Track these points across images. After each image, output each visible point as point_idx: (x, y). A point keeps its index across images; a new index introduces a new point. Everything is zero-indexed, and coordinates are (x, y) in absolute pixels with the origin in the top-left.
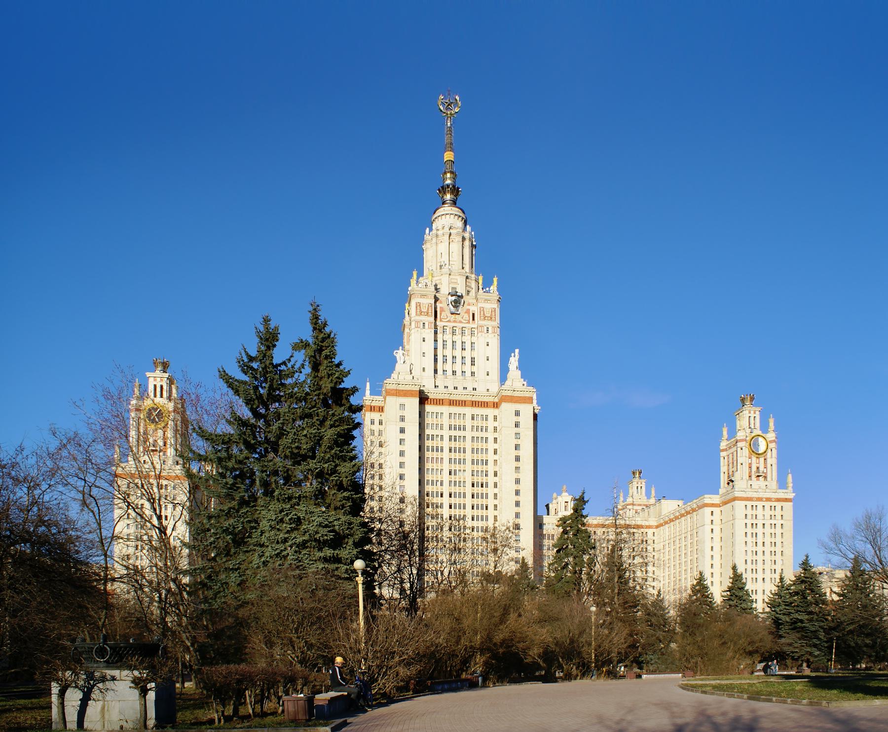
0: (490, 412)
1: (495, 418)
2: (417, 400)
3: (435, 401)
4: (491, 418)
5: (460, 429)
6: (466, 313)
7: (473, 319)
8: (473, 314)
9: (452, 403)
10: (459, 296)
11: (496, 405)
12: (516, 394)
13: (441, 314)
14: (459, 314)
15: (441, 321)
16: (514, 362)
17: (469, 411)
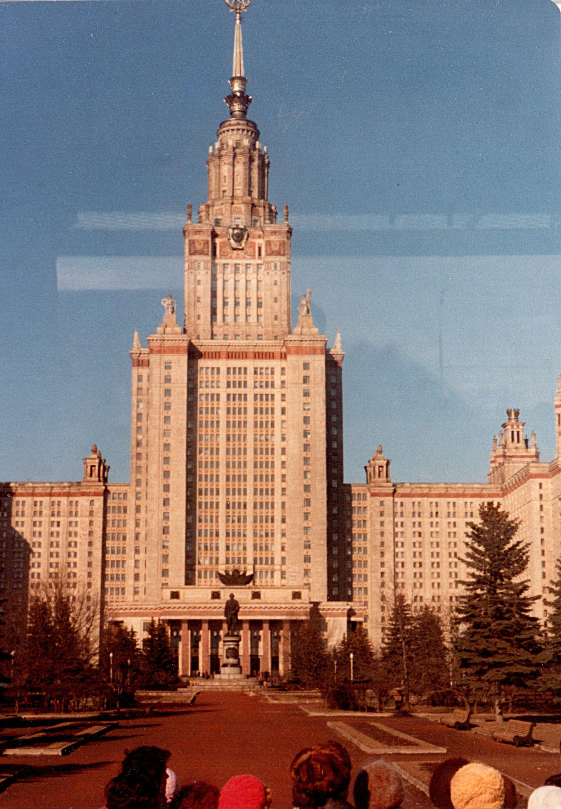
0: (276, 364)
2: (184, 358)
3: (210, 354)
4: (278, 371)
6: (250, 247)
7: (260, 254)
8: (260, 249)
9: (230, 356)
10: (241, 229)
11: (283, 356)
13: (221, 251)
17: (250, 364)
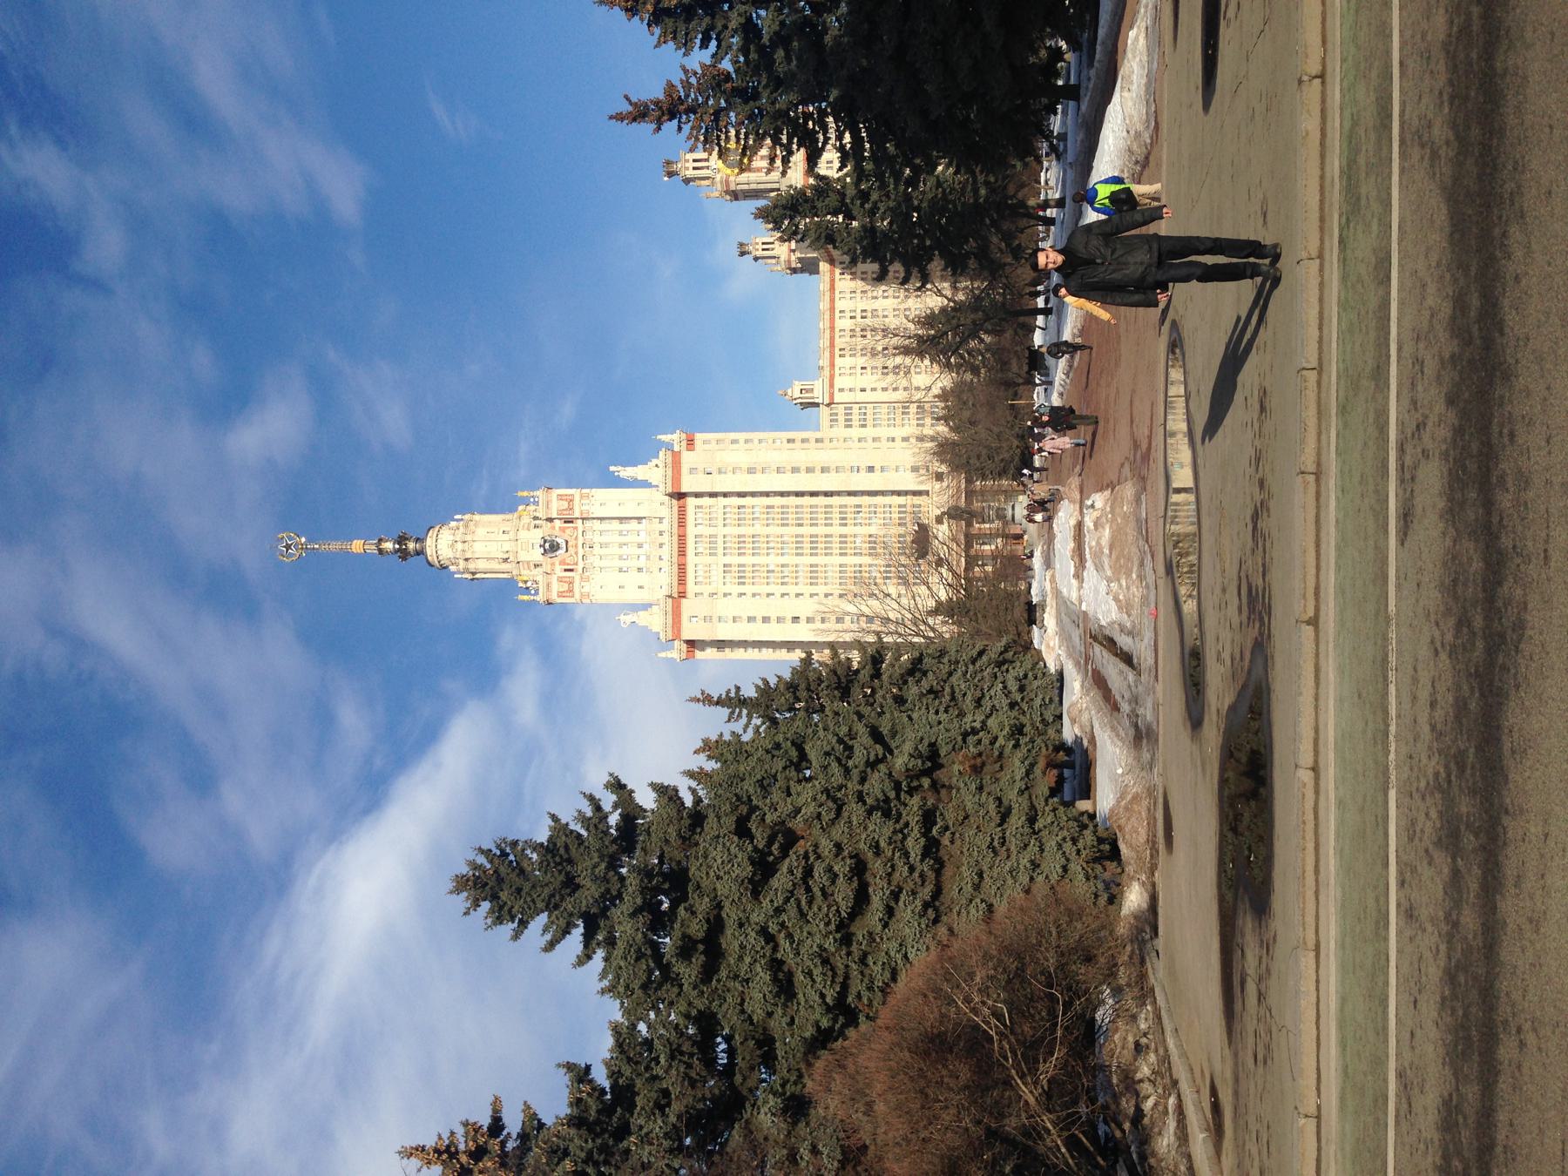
1: (697, 495)
2: (683, 600)
4: (699, 501)
5: (716, 543)
9: (682, 552)
10: (545, 541)
11: (681, 496)
12: (669, 473)
14: (567, 542)
15: (576, 564)
16: (627, 472)
17: (691, 531)
